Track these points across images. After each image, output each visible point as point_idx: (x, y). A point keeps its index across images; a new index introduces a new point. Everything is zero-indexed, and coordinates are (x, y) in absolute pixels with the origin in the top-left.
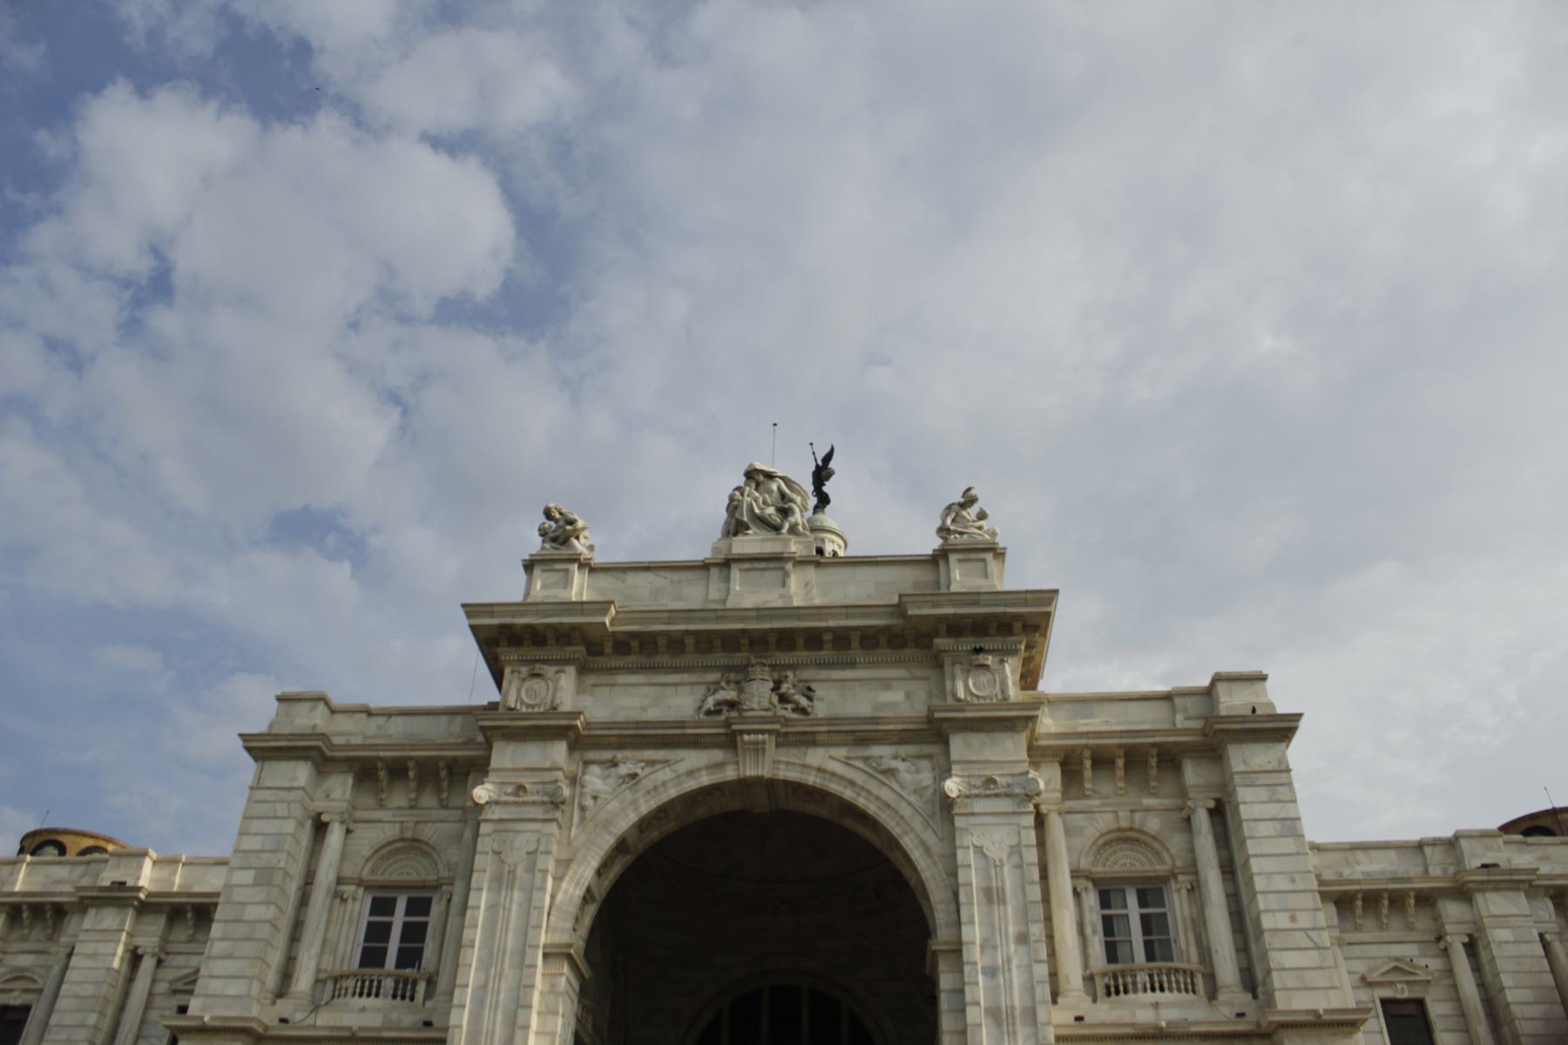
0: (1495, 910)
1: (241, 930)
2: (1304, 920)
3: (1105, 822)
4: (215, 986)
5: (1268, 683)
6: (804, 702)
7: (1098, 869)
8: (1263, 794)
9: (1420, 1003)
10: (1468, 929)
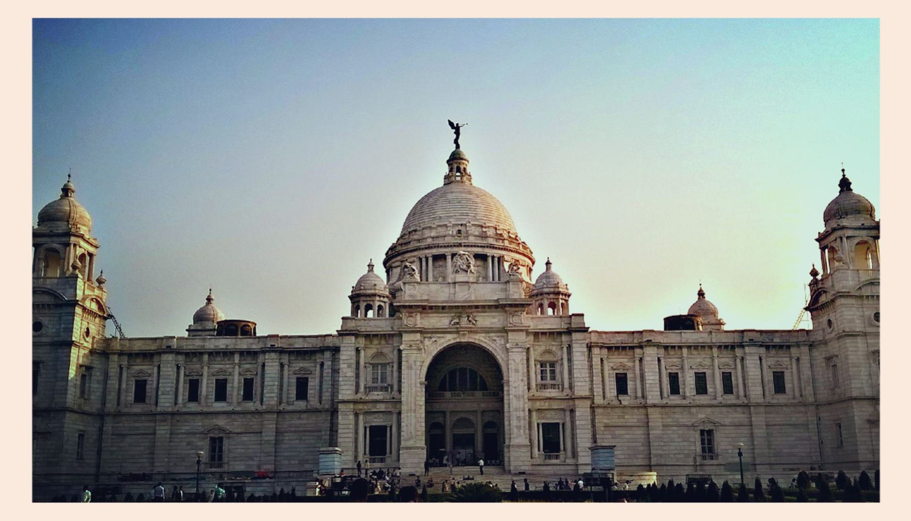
1: (346, 379)
2: (584, 375)
3: (543, 348)
4: (344, 392)
5: (585, 317)
6: (474, 322)
7: (541, 359)
8: (579, 345)
9: (626, 374)
10: (641, 356)
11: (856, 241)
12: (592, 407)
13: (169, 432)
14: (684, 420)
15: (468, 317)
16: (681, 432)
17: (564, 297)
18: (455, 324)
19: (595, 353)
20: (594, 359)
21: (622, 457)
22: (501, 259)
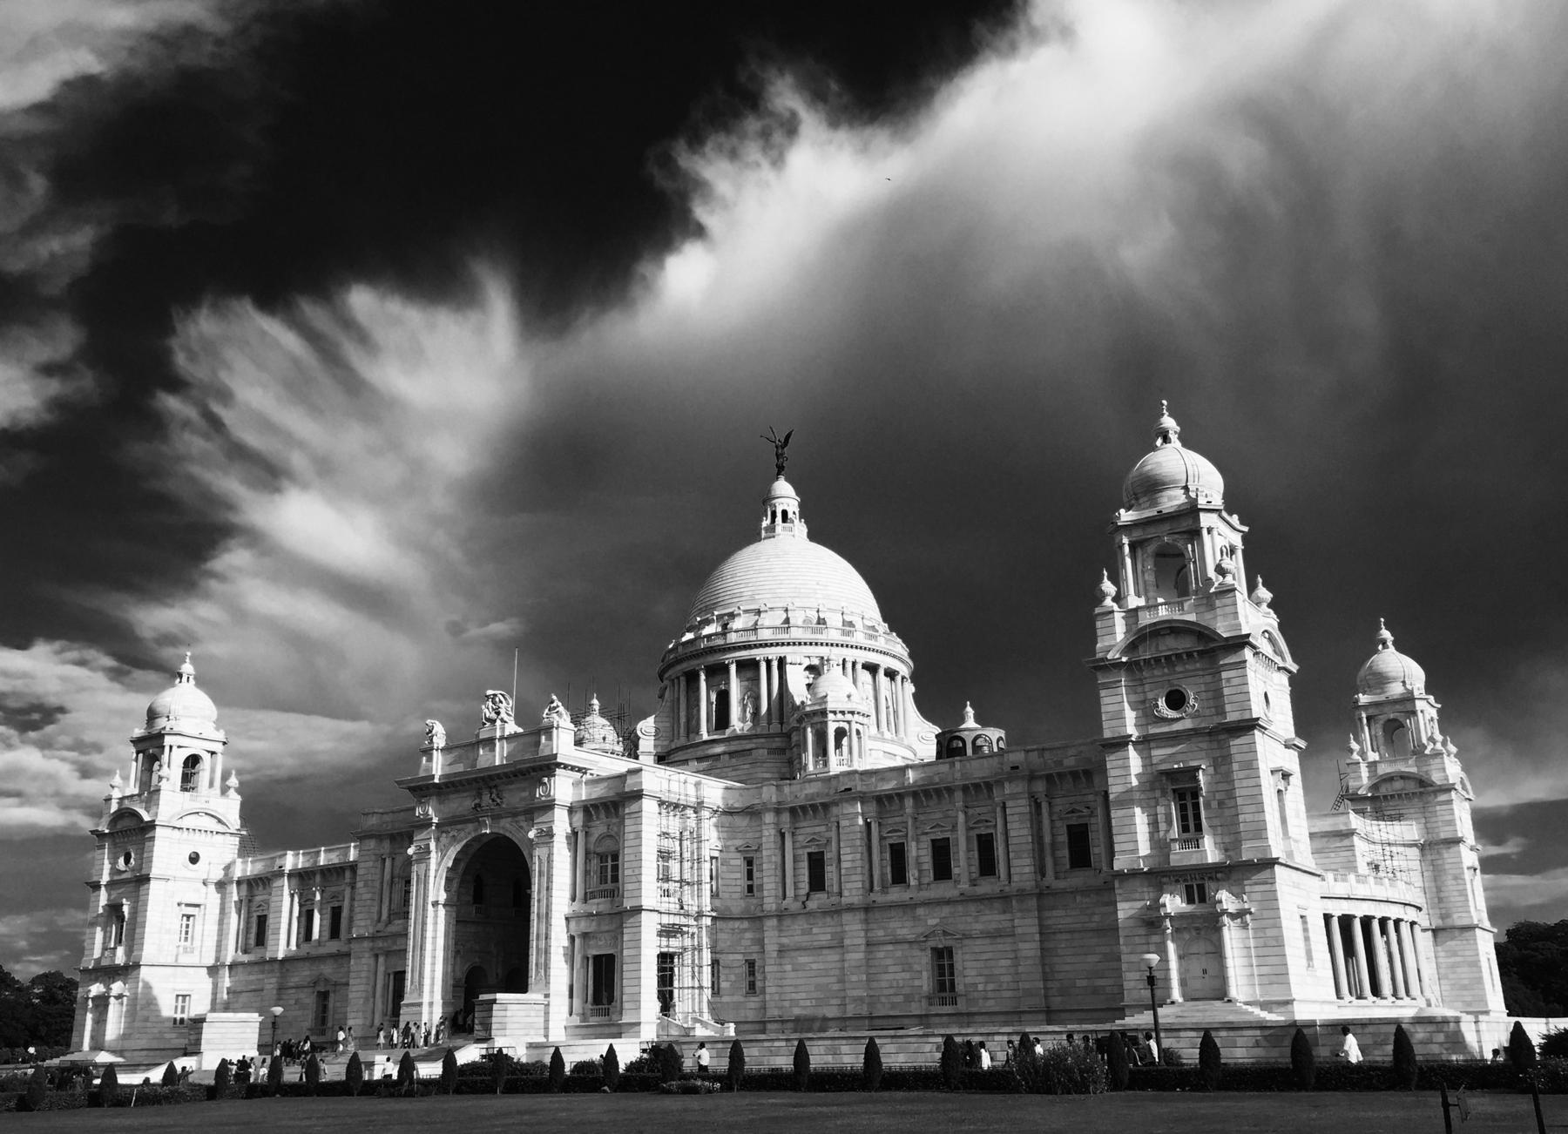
0: (845, 812)
6: (499, 801)
7: (599, 850)
9: (823, 852)
11: (1151, 548)
12: (756, 919)
13: (276, 986)
14: (905, 931)
15: (491, 794)
16: (899, 954)
17: (840, 716)
18: (475, 808)
19: (767, 822)
20: (766, 833)
21: (808, 1003)
22: (782, 662)
